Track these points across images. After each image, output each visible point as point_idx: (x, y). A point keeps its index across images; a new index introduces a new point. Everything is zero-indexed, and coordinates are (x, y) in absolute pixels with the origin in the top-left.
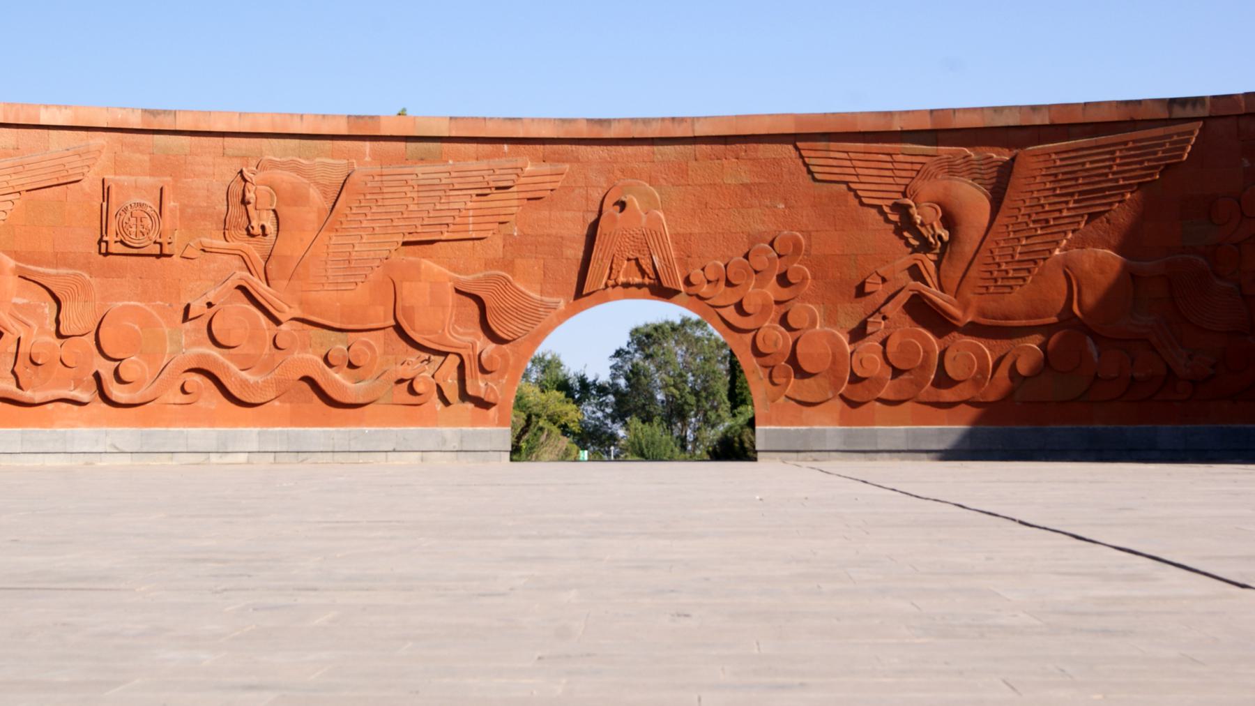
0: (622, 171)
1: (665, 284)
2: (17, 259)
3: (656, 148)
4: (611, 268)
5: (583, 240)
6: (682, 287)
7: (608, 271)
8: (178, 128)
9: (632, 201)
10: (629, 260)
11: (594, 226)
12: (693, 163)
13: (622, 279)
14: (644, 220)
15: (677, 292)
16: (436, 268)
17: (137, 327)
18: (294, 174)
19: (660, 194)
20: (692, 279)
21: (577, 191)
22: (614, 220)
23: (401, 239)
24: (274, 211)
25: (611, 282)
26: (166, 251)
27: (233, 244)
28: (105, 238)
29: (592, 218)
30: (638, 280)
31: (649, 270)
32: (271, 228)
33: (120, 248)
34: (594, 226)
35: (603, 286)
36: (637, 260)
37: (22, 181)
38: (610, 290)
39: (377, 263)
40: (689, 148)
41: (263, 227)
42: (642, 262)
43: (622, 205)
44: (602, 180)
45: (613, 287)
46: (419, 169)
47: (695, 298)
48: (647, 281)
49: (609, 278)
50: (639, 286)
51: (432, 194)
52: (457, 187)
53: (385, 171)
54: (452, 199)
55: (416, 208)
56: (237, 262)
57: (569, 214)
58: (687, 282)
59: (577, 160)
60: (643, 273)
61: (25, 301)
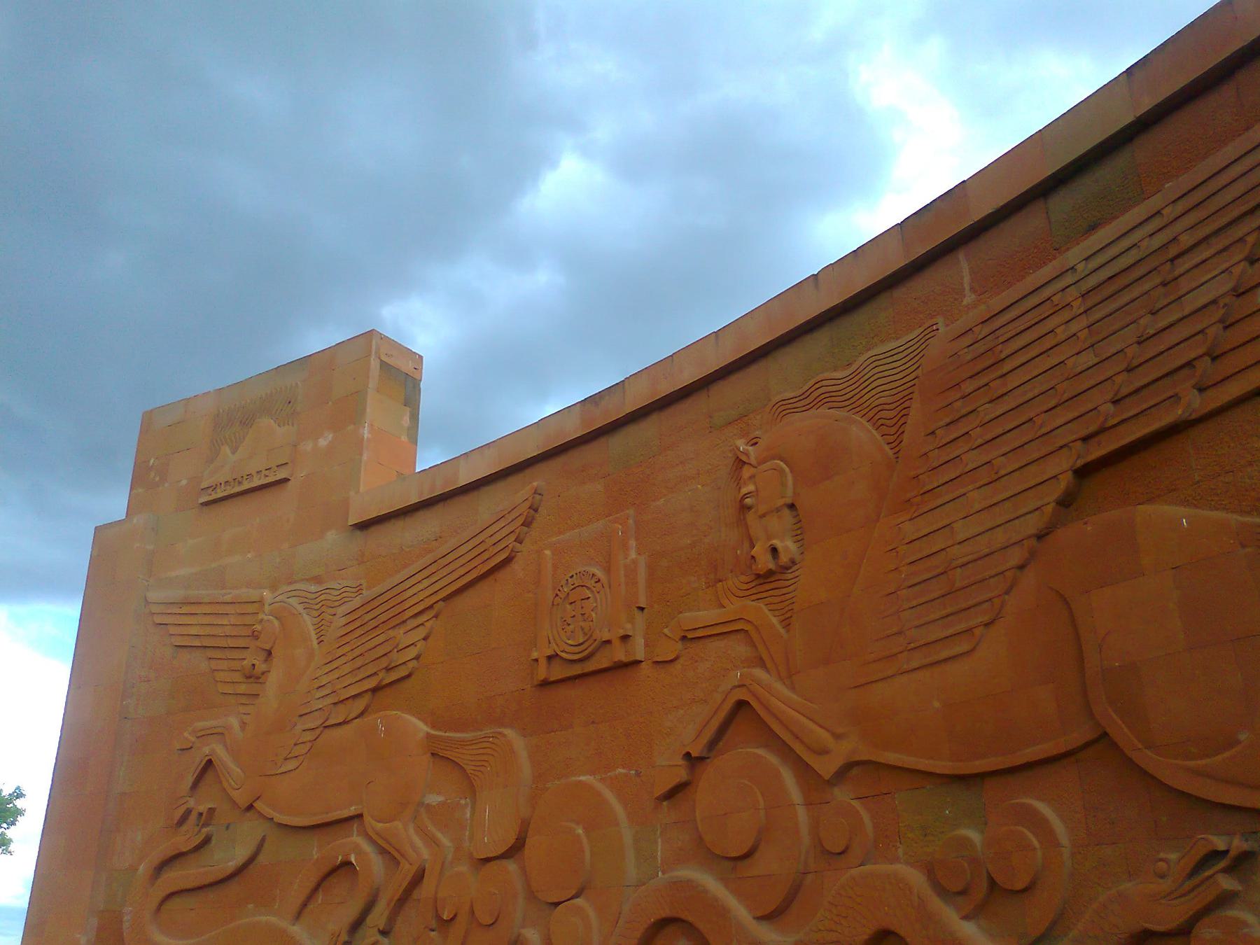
2: (433, 727)
8: (629, 409)
16: (1184, 516)
17: (580, 831)
18: (824, 410)
23: (1063, 465)
24: (792, 506)
26: (620, 655)
27: (733, 607)
28: (535, 655)
32: (788, 546)
33: (558, 672)
37: (437, 587)
39: (1016, 556)
41: (774, 550)
46: (1074, 255)
51: (1126, 297)
52: (1187, 240)
53: (997, 302)
54: (1184, 285)
55: (1088, 359)
56: (740, 649)
61: (441, 799)
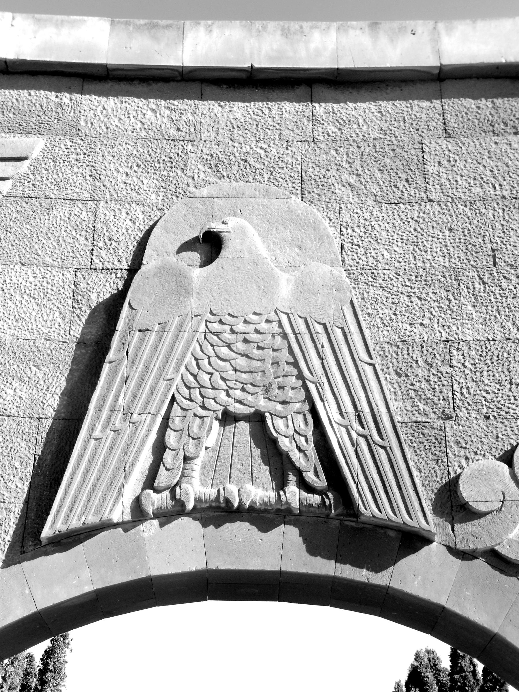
0: (215, 166)
1: (368, 509)
3: (320, 109)
4: (160, 448)
5: (67, 355)
6: (430, 523)
7: (146, 458)
9: (243, 231)
10: (228, 418)
11: (110, 310)
12: (436, 145)
13: (197, 489)
14: (285, 288)
15: (413, 541)
19: (341, 226)
20: (466, 491)
21: (62, 211)
22: (182, 287)
25: (155, 501)
29: (102, 289)
30: (260, 492)
31: (305, 459)
34: (110, 310)
35: (121, 512)
36: (258, 420)
38: (150, 528)
40: (423, 110)
42: (278, 427)
43: (211, 245)
44: (149, 183)
45: (165, 517)
47: (480, 563)
48: (294, 495)
49: (150, 482)
50: (264, 518)
57: (28, 277)
58: (452, 503)
59: (74, 129)
60: (280, 466)
